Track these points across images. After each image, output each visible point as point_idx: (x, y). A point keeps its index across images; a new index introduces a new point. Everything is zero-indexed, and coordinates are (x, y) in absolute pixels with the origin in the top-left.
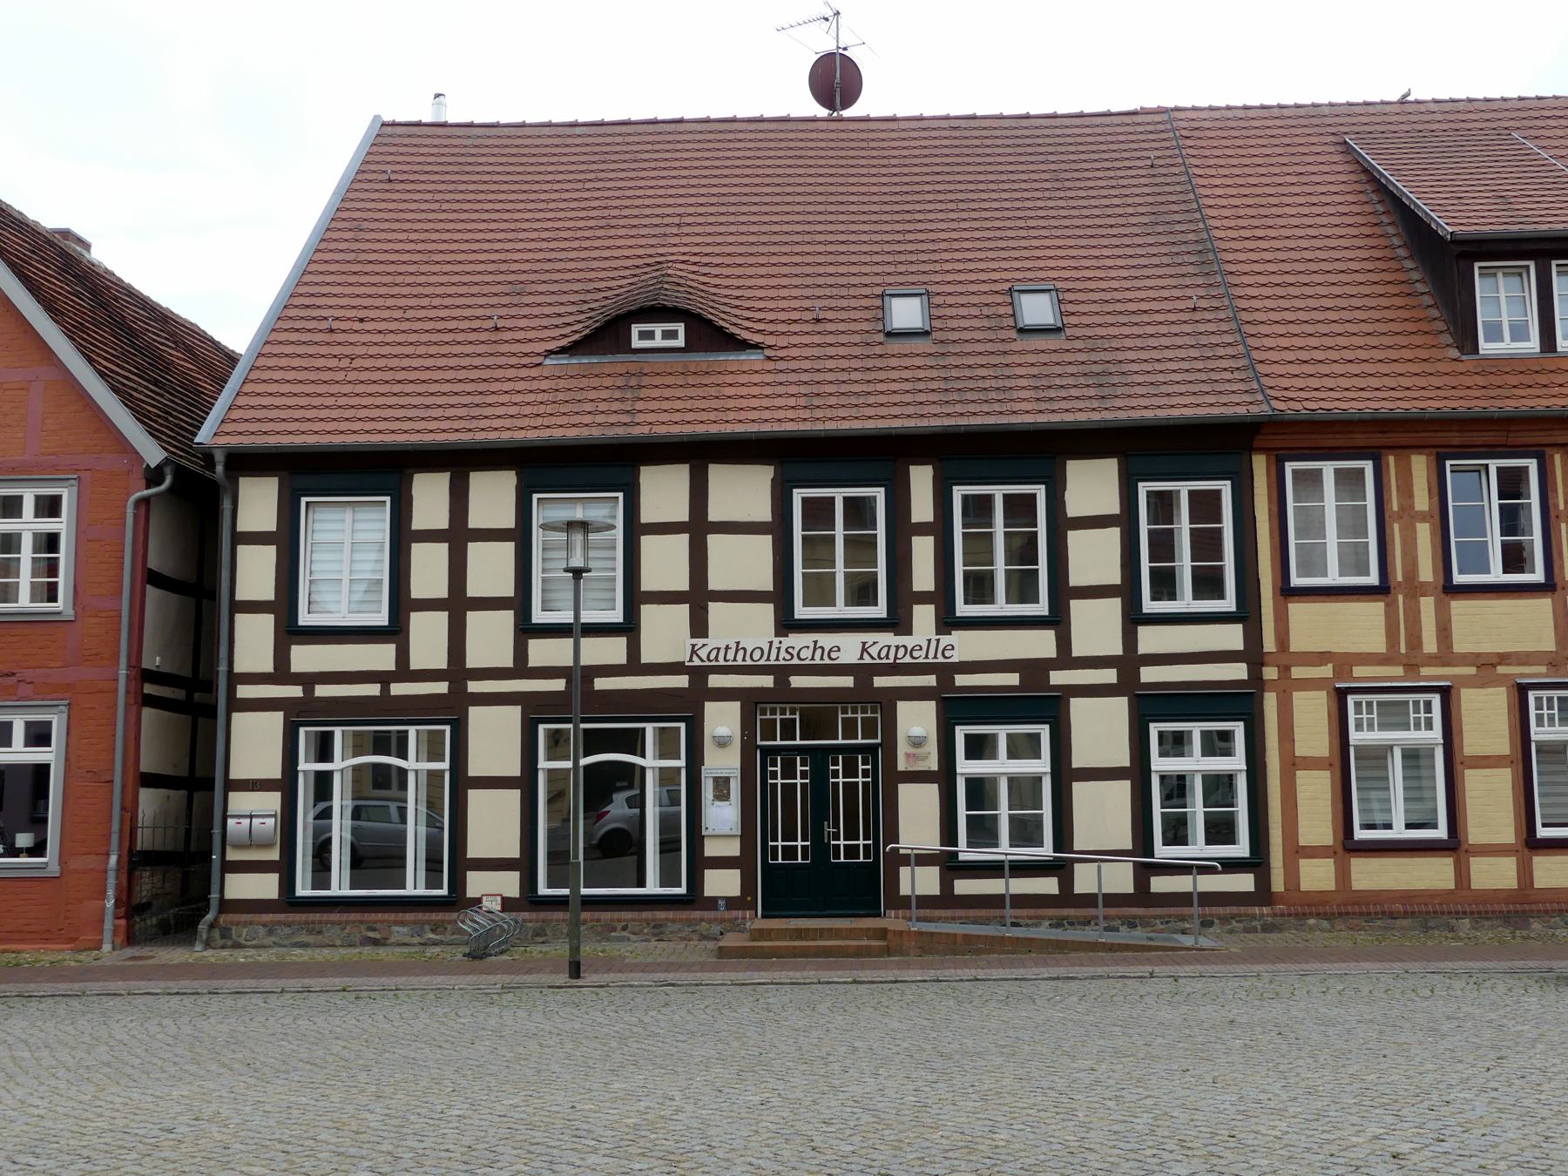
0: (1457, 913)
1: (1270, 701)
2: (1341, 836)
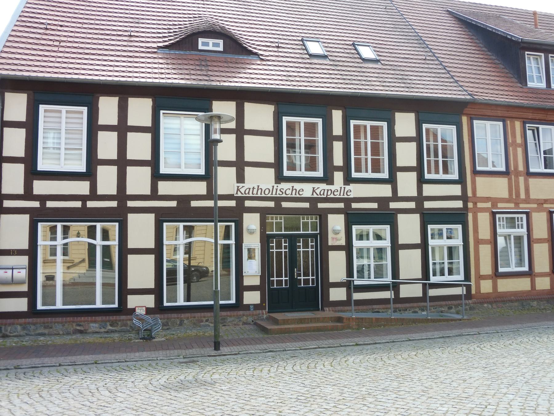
0: (533, 299)
1: (470, 216)
2: (494, 271)
